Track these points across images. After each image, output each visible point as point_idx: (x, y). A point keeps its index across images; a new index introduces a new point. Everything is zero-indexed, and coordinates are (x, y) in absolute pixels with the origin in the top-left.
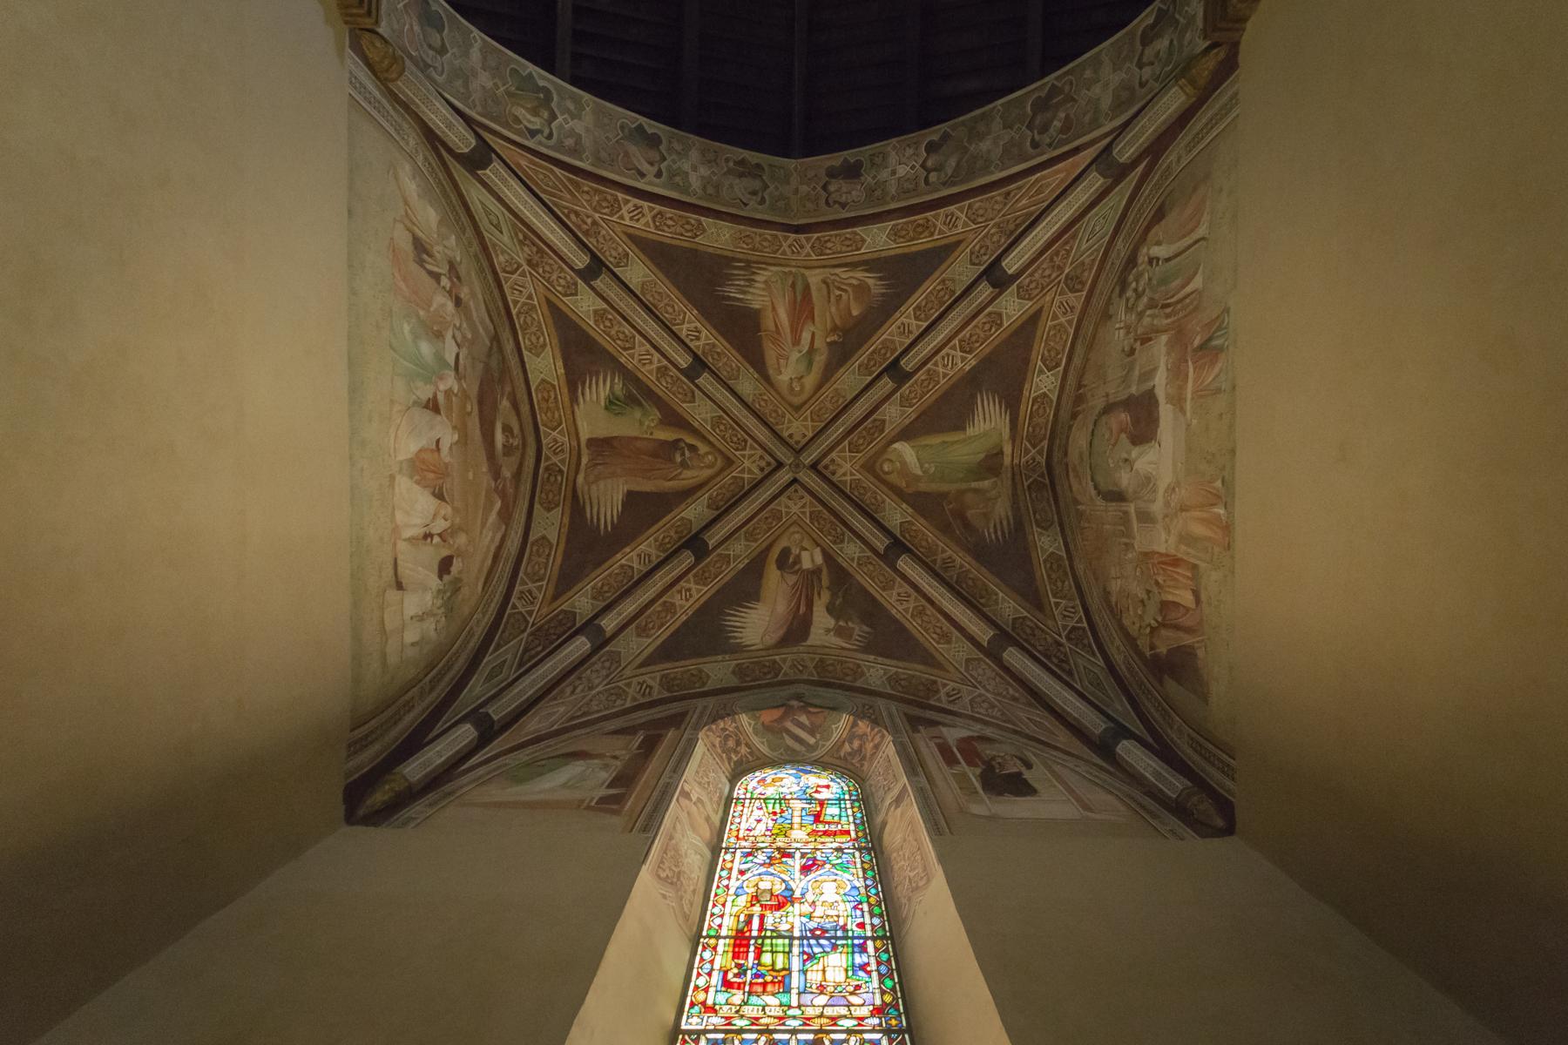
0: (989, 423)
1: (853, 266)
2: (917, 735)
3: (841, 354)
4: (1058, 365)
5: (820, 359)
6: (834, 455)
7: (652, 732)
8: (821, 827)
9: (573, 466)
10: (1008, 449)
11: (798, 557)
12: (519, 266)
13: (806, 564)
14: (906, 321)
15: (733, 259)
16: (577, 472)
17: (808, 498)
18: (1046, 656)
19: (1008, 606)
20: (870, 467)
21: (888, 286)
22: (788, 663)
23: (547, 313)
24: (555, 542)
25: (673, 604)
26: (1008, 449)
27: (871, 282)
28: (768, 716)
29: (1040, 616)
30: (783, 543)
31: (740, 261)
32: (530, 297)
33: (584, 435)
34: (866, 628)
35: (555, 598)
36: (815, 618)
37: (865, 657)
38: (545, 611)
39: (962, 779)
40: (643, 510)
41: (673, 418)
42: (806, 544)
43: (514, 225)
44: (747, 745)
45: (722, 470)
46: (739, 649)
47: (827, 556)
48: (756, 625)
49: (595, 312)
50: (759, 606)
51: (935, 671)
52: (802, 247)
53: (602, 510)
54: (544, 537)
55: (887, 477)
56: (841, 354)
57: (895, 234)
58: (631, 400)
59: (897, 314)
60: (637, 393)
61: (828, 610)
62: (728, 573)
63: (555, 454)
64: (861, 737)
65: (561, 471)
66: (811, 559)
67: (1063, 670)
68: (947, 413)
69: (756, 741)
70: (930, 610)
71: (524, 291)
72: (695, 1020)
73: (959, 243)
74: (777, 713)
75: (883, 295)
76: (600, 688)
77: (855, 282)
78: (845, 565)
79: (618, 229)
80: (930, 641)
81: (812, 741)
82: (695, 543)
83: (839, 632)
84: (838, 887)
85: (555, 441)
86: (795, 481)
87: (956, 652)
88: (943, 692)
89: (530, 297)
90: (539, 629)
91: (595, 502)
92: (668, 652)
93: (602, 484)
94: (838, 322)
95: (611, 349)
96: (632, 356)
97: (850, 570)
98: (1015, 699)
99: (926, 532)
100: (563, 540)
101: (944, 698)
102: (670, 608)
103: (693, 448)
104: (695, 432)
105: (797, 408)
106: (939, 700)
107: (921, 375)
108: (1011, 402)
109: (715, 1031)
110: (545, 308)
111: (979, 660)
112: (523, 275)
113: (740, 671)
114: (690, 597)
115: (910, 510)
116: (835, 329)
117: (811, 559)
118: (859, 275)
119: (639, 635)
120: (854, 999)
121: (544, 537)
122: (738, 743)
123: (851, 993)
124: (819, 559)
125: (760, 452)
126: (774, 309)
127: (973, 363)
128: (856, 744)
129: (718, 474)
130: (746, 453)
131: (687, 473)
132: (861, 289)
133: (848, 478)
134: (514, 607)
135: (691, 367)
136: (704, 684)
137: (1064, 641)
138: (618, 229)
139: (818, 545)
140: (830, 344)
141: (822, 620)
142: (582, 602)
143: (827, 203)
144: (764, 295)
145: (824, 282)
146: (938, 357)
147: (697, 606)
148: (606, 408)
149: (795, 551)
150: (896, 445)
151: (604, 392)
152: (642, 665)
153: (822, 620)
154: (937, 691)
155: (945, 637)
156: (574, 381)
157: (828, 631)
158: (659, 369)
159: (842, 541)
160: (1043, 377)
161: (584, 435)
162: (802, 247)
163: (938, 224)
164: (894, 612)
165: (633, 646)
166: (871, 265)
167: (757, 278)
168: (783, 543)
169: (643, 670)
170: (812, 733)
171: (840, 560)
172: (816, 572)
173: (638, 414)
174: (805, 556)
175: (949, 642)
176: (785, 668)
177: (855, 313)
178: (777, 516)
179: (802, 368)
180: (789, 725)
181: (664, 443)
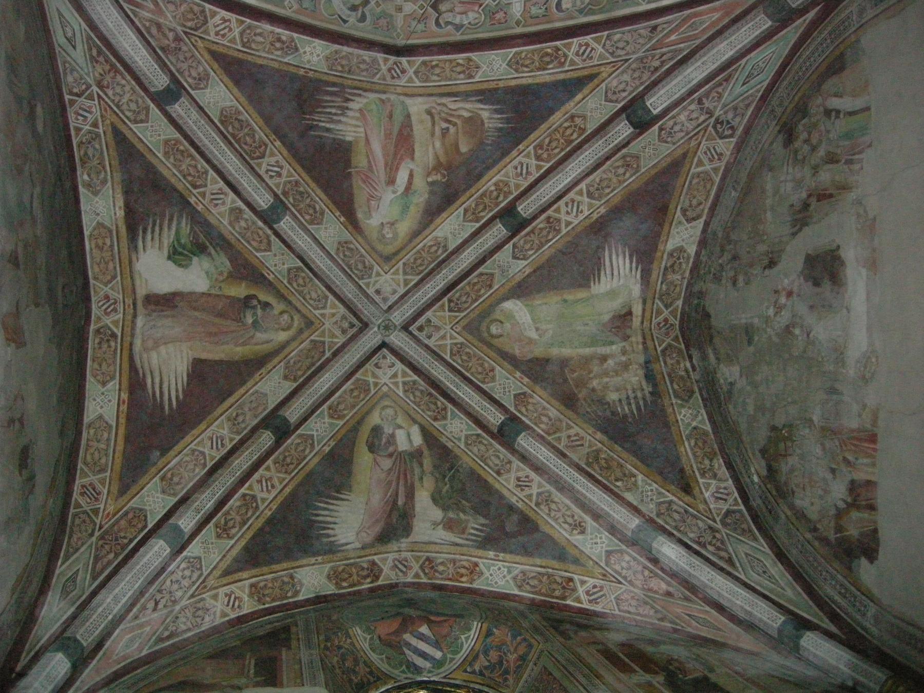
0: (619, 280)
1: (466, 96)
3: (444, 200)
4: (698, 217)
5: (420, 199)
6: (429, 314)
9: (128, 330)
10: (637, 310)
11: (393, 436)
12: (89, 87)
13: (402, 444)
14: (525, 160)
15: (328, 84)
16: (133, 336)
17: (399, 366)
18: (699, 543)
19: (649, 491)
20: (473, 328)
21: (508, 121)
22: (390, 563)
23: (112, 143)
24: (114, 424)
25: (254, 497)
26: (637, 310)
27: (485, 115)
28: (385, 629)
29: (687, 498)
30: (375, 419)
31: (334, 84)
32: (95, 125)
33: (141, 292)
34: (482, 521)
35: (123, 491)
36: (418, 508)
37: (480, 552)
38: (111, 509)
40: (213, 382)
41: (246, 270)
42: (399, 421)
43: (89, 38)
45: (301, 331)
46: (332, 549)
47: (425, 432)
48: (349, 522)
49: (166, 142)
50: (352, 497)
51: (572, 568)
52: (403, 71)
53: (165, 386)
54: (101, 417)
55: (495, 342)
56: (444, 200)
57: (516, 64)
58: (200, 249)
59: (514, 153)
60: (202, 241)
61: (434, 500)
62: (312, 460)
63: (107, 314)
65: (114, 335)
66: (408, 438)
67: (721, 558)
68: (573, 266)
69: (374, 657)
70: (557, 496)
71: (86, 117)
73: (591, 77)
74: (395, 625)
75: (500, 130)
76: (184, 602)
77: (466, 114)
78: (450, 445)
79: (200, 44)
80: (561, 532)
81: (438, 655)
82: (278, 426)
83: (449, 525)
85: (107, 297)
86: (384, 345)
87: (594, 543)
88: (581, 591)
89: (95, 125)
90: (106, 532)
91: (157, 374)
92: (255, 555)
93: (163, 349)
94: (443, 159)
95: (180, 187)
96: (203, 195)
97: (456, 450)
98: (669, 594)
99: (543, 406)
100: (123, 421)
101: (583, 597)
102: (250, 501)
103: (266, 305)
104: (270, 286)
105: (388, 259)
106: (578, 600)
107: (540, 223)
108: (645, 254)
110: (110, 136)
111: (621, 552)
112: (91, 97)
113: (335, 576)
114: (269, 490)
115: (526, 380)
116: (438, 166)
117: (408, 438)
118: (468, 106)
119: (219, 536)
121: (101, 417)
122: (356, 661)
124: (418, 440)
125: (342, 310)
126: (367, 141)
127: (603, 210)
128: (494, 655)
129: (293, 339)
130: (328, 311)
131: (260, 336)
132: (473, 122)
133: (449, 342)
134: (78, 505)
135: (272, 208)
136: (297, 593)
137: (719, 526)
138: (200, 44)
139: (415, 421)
140: (432, 184)
141: (427, 512)
142: (153, 499)
143: (438, 24)
144: (355, 125)
145: (429, 112)
146: (561, 203)
147: (280, 499)
148: (169, 258)
149: (388, 430)
150: (508, 305)
151: (168, 237)
152: (227, 573)
153: (427, 512)
154: (574, 590)
155: (580, 527)
156: (135, 223)
157: (435, 524)
158: (232, 210)
159: (445, 418)
160: (681, 228)
161: (141, 292)
162: (403, 71)
163: (571, 55)
164: (514, 500)
165: (211, 550)
166: (486, 95)
167: (351, 105)
168: (375, 419)
169: (229, 579)
170: (437, 645)
171: (443, 440)
172: (417, 455)
173: (206, 263)
174: (400, 435)
175: (582, 532)
176: (386, 569)
177: (464, 149)
178: (364, 387)
179: (395, 211)
180: (407, 637)
181: (233, 300)
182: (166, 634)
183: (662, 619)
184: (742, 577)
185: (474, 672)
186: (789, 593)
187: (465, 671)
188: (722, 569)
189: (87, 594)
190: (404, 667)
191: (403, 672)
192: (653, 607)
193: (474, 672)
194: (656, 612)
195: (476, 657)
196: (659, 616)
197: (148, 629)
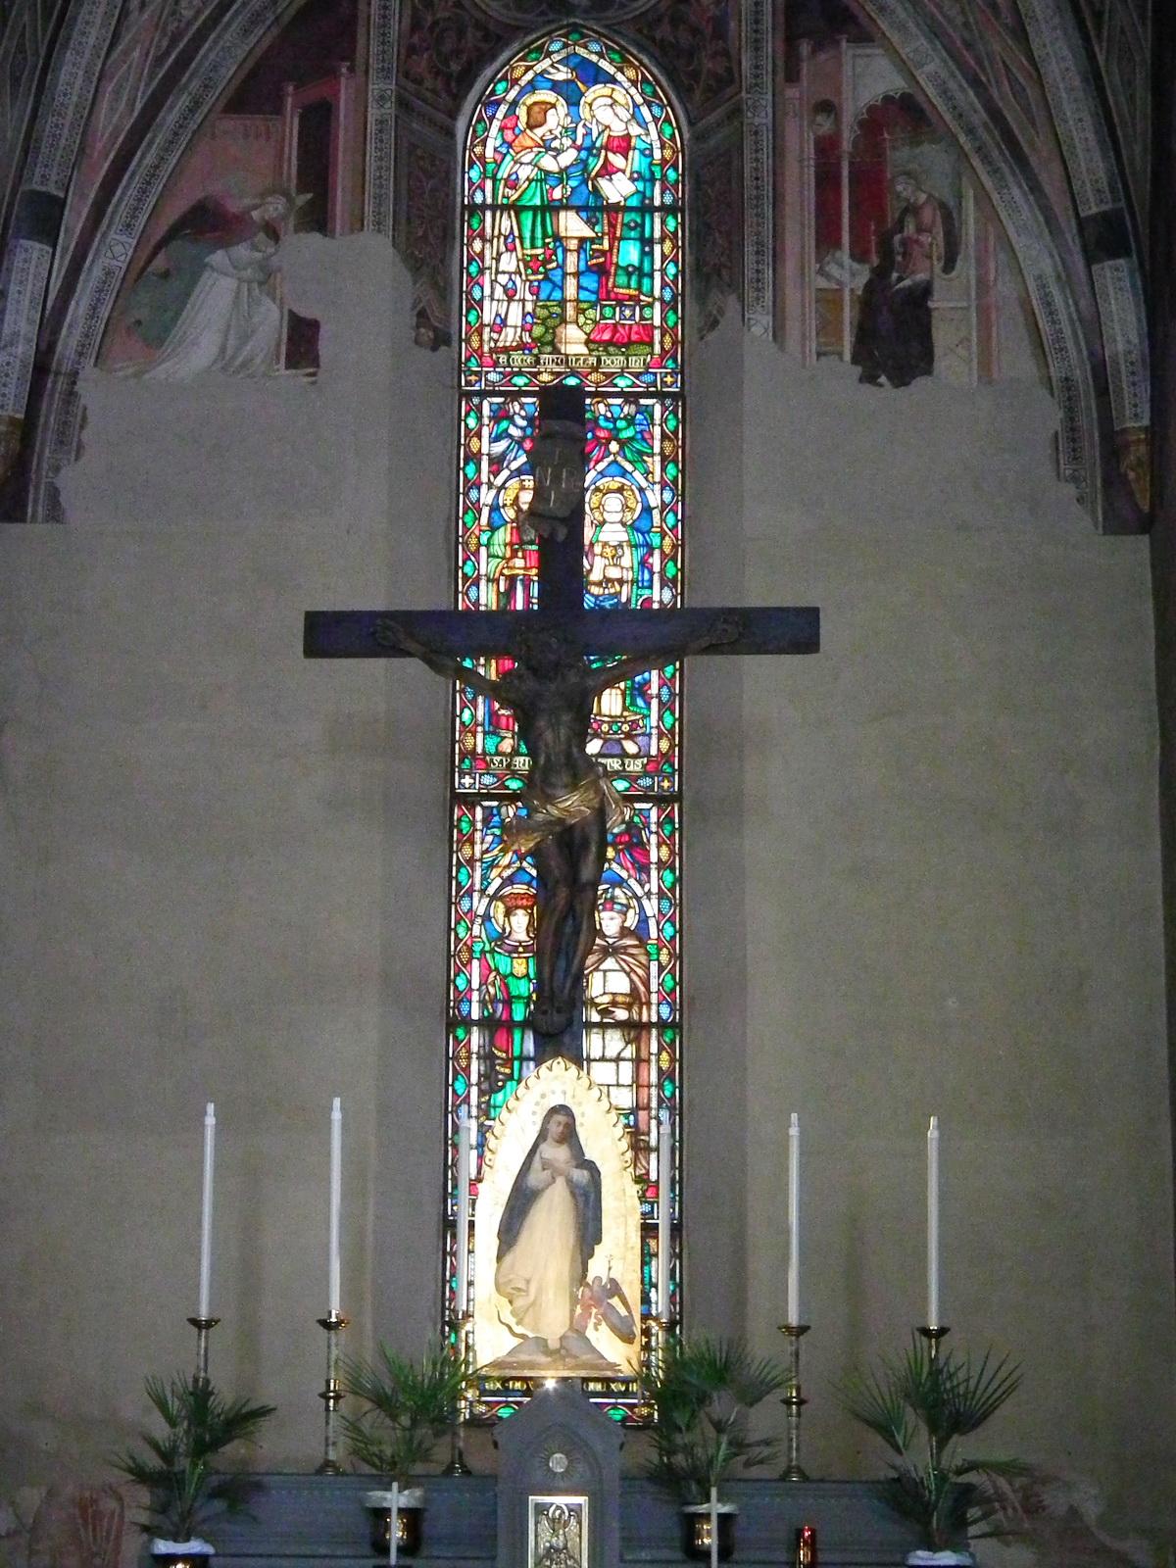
2: (791, 92)
7: (314, 93)
8: (611, 314)
39: (829, 300)
44: (478, 25)
64: (695, 31)
72: (467, 781)
84: (625, 507)
109: (490, 797)
120: (630, 747)
123: (629, 736)
182: (165, 43)
183: (969, 46)
184: (1101, 58)
185: (653, 39)
186: (1138, 149)
187: (640, 31)
188: (1081, 25)
189: (43, 52)
190: (544, 6)
191: (543, 13)
192: (963, 12)
193: (653, 39)
194: (966, 24)
195: (659, 20)
196: (967, 35)
197: (136, 54)
